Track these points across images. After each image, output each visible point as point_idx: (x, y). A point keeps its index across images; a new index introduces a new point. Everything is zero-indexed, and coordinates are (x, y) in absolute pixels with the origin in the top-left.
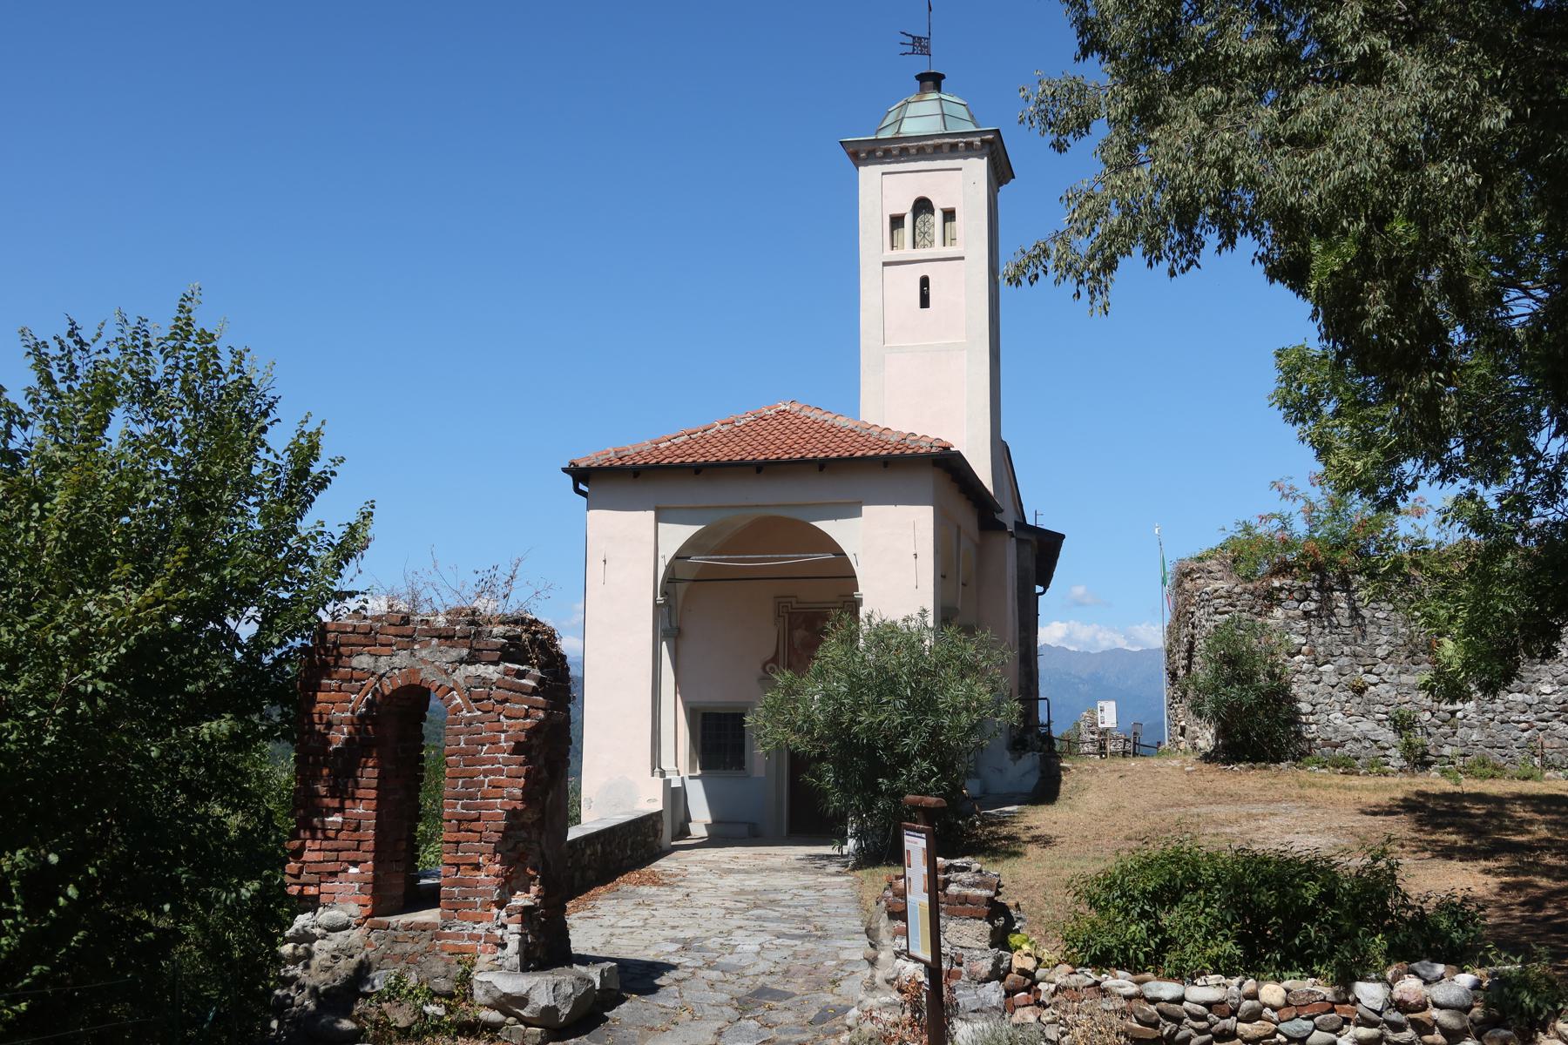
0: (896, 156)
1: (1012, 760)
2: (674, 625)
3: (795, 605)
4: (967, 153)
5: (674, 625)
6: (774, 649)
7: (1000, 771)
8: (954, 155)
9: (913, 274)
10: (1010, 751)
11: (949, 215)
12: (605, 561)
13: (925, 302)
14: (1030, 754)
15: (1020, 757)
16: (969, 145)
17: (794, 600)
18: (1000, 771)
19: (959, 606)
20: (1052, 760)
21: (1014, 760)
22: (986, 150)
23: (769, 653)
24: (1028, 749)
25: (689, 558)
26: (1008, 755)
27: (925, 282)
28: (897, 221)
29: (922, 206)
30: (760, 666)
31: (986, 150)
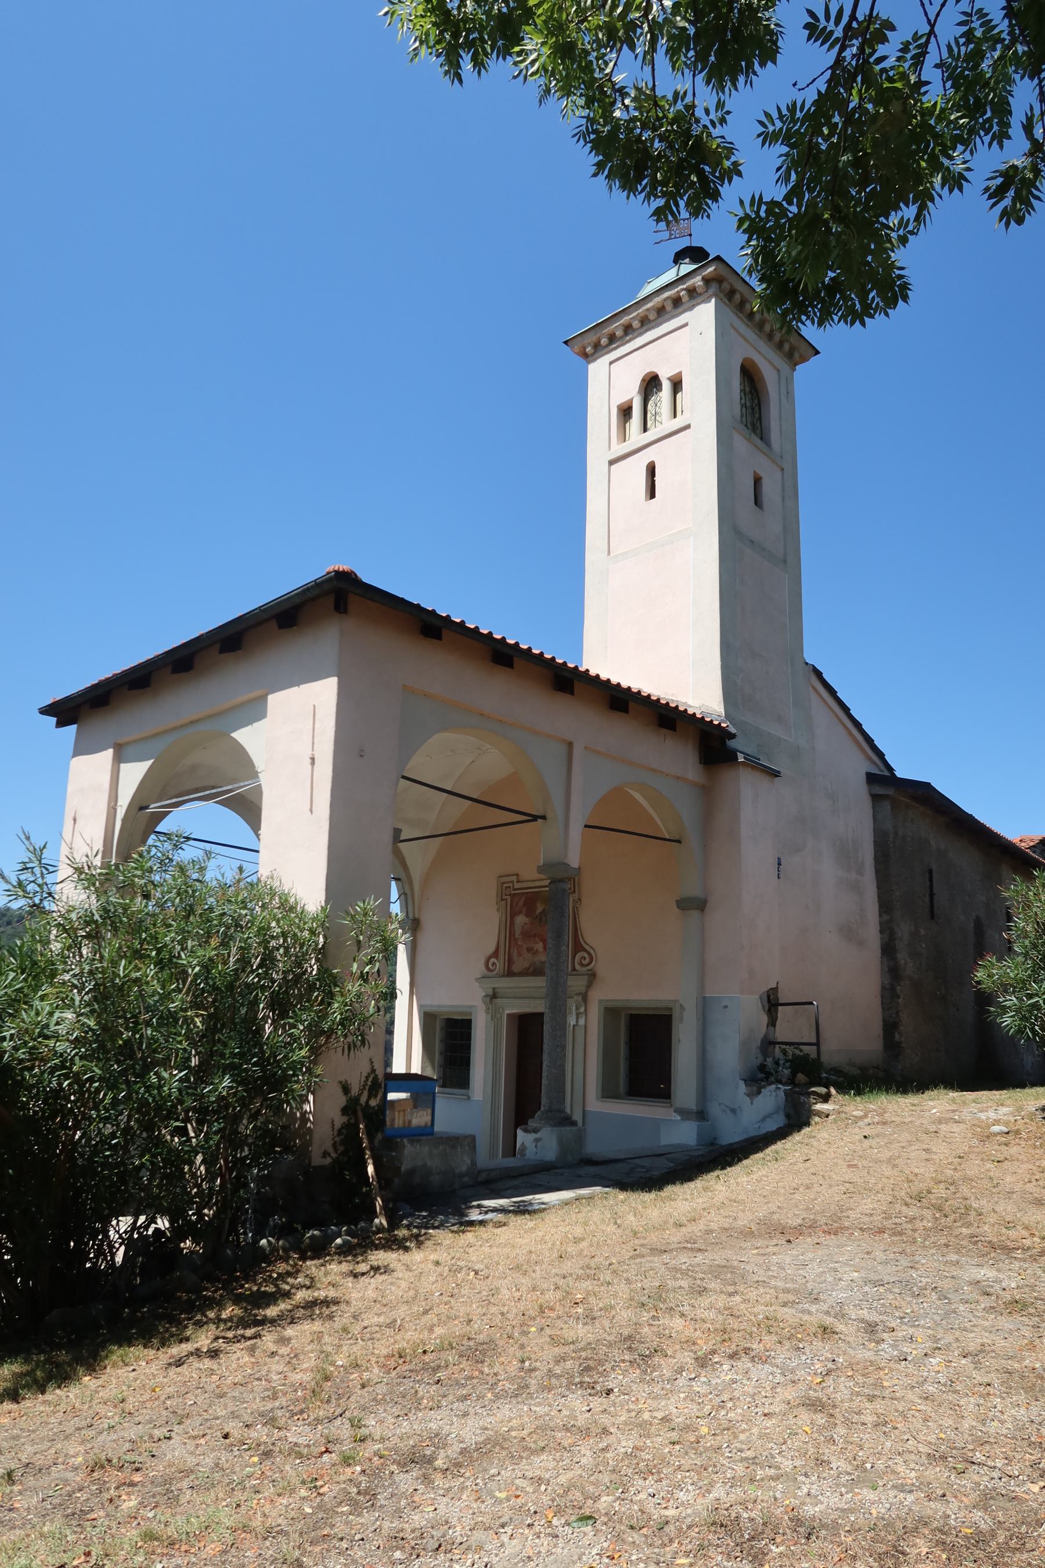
0: (621, 338)
1: (748, 1095)
2: (411, 916)
3: (517, 886)
4: (694, 302)
5: (411, 916)
6: (496, 941)
7: (733, 1111)
8: (680, 309)
9: (636, 467)
10: (745, 1081)
11: (677, 385)
12: (75, 820)
13: (652, 492)
14: (773, 1087)
15: (759, 1092)
16: (692, 292)
17: (514, 878)
18: (733, 1111)
19: (574, 861)
20: (802, 1098)
21: (752, 1095)
22: (713, 289)
23: (491, 949)
24: (772, 1079)
25: (147, 807)
26: (742, 1087)
27: (651, 470)
28: (626, 412)
29: (651, 384)
30: (483, 961)
31: (713, 289)
